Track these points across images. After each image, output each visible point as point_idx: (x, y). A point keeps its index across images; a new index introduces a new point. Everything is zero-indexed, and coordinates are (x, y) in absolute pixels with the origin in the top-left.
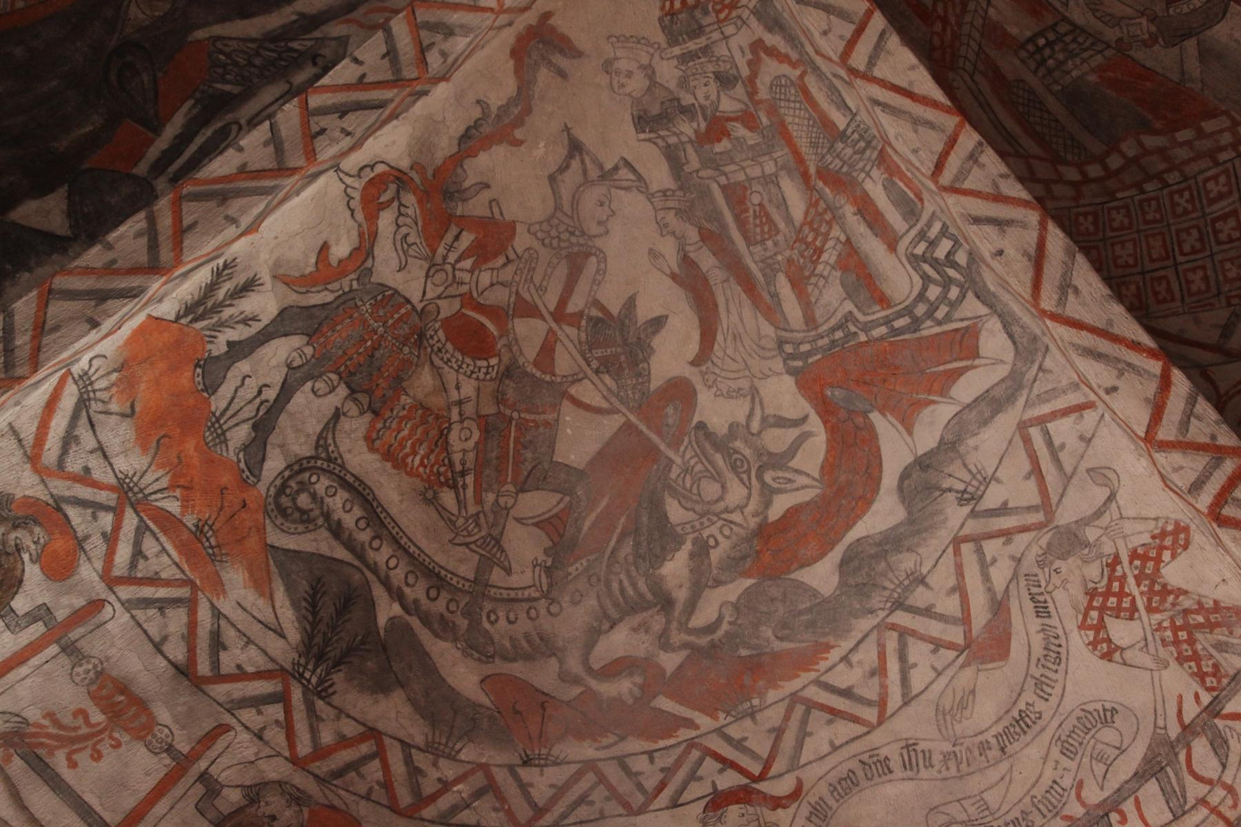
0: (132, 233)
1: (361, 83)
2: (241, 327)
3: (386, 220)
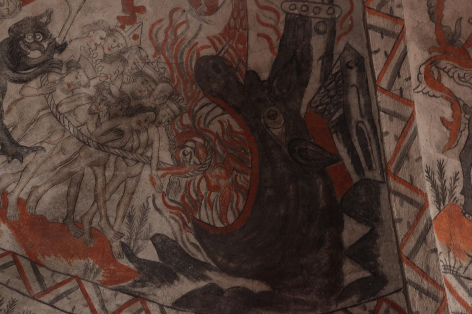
0: (399, 207)
1: (389, 57)
2: (457, 183)
3: (446, 82)
